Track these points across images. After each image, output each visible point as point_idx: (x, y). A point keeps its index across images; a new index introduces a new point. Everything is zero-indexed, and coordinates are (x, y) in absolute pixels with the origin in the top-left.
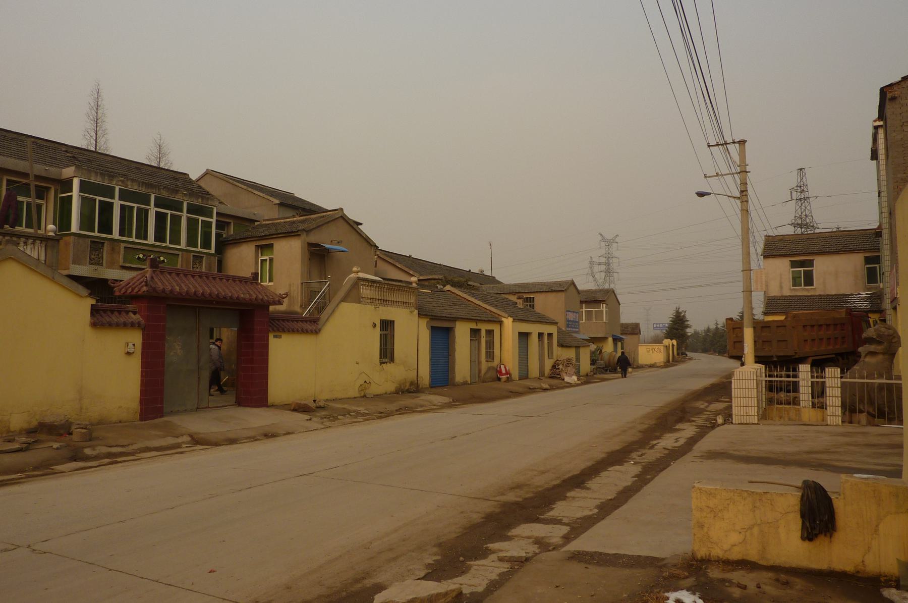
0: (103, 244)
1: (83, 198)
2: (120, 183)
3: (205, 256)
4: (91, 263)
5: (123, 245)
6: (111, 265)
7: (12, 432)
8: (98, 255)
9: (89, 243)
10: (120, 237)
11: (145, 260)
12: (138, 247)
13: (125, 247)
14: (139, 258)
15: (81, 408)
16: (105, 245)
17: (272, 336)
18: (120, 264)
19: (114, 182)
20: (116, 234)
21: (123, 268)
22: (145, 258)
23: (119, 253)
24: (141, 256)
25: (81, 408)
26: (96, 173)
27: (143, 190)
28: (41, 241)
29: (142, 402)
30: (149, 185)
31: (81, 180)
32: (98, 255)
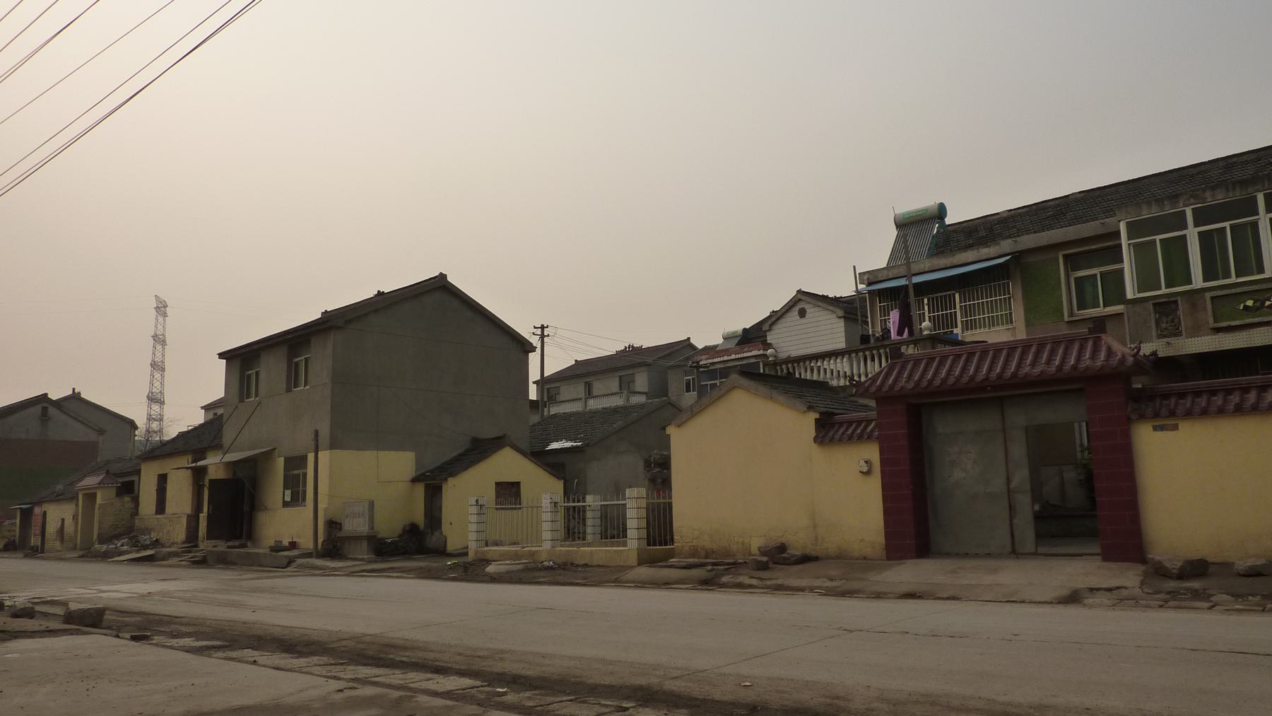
0: (1176, 302)
1: (1137, 247)
2: (1192, 201)
3: (1179, 298)
4: (1160, 336)
5: (1208, 295)
6: (1196, 331)
7: (753, 555)
8: (1172, 321)
9: (1151, 308)
10: (1205, 284)
11: (1258, 309)
12: (1238, 290)
13: (1212, 298)
14: (1246, 307)
15: (816, 538)
16: (1179, 302)
17: (1151, 428)
18: (1211, 326)
19: (1181, 204)
20: (1198, 281)
21: (1218, 330)
22: (1258, 304)
23: (1205, 308)
24: (1250, 303)
25: (816, 538)
26: (1149, 204)
27: (1238, 194)
28: (915, 345)
29: (888, 535)
30: (1243, 183)
31: (1127, 222)
32: (1172, 321)
